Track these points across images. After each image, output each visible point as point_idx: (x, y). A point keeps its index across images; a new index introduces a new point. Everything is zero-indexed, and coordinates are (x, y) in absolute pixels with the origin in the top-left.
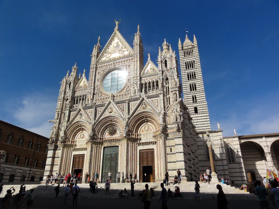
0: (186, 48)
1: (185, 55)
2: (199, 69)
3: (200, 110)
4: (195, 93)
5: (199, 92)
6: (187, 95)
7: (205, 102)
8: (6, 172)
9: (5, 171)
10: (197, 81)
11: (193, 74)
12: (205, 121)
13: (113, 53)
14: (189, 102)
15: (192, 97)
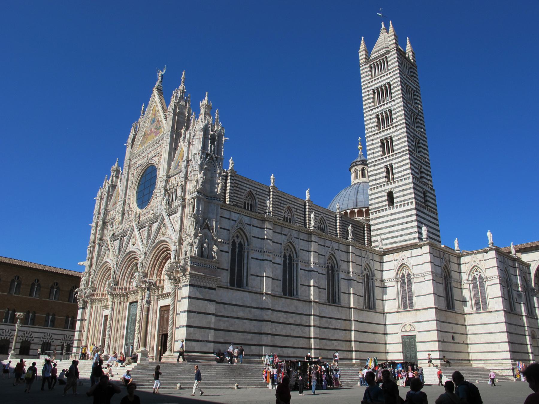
0: (375, 55)
1: (371, 75)
2: (398, 101)
3: (398, 197)
4: (391, 158)
5: (398, 155)
6: (375, 165)
7: (409, 177)
8: (55, 341)
9: (53, 339)
10: (395, 129)
11: (388, 113)
12: (407, 223)
13: (148, 135)
14: (377, 182)
15: (384, 169)
